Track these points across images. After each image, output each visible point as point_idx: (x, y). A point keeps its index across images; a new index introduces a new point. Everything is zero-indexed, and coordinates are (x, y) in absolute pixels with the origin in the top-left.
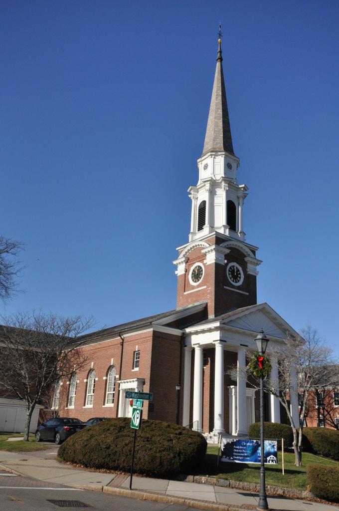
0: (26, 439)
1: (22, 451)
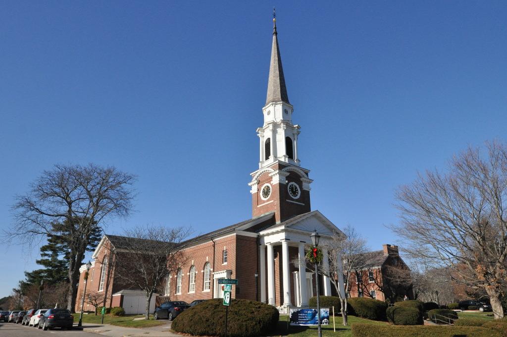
0: (147, 318)
1: (145, 327)
